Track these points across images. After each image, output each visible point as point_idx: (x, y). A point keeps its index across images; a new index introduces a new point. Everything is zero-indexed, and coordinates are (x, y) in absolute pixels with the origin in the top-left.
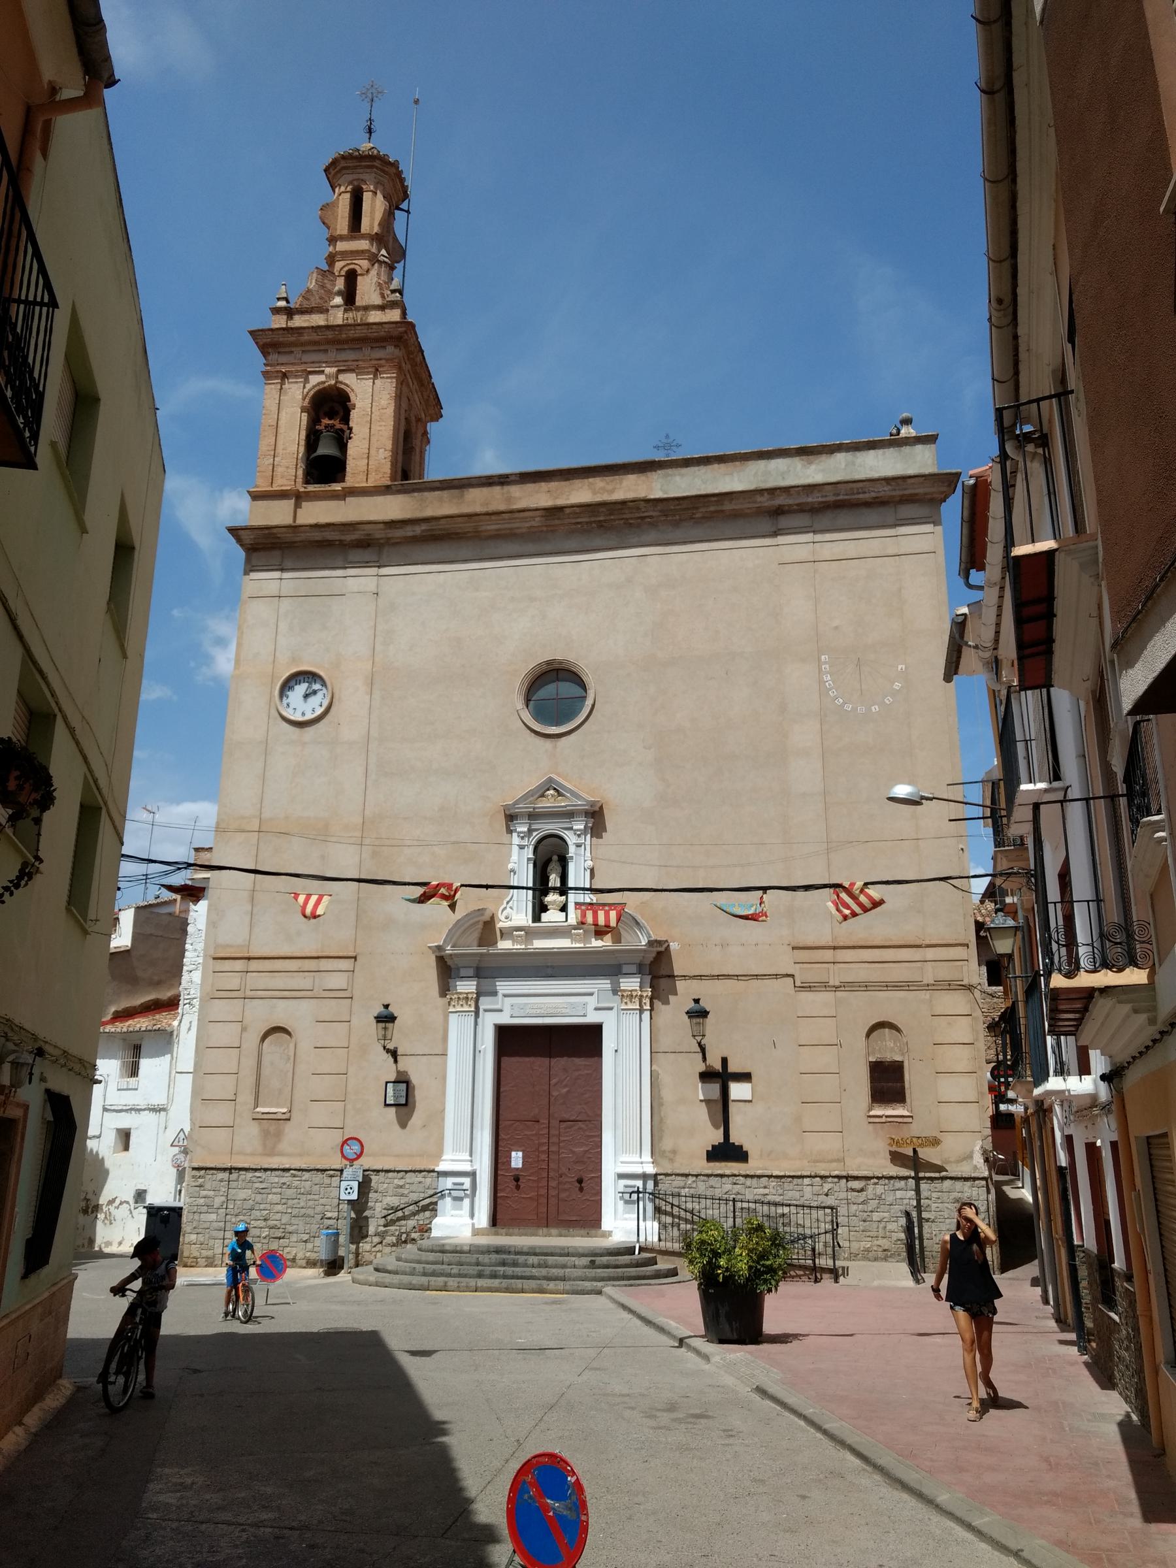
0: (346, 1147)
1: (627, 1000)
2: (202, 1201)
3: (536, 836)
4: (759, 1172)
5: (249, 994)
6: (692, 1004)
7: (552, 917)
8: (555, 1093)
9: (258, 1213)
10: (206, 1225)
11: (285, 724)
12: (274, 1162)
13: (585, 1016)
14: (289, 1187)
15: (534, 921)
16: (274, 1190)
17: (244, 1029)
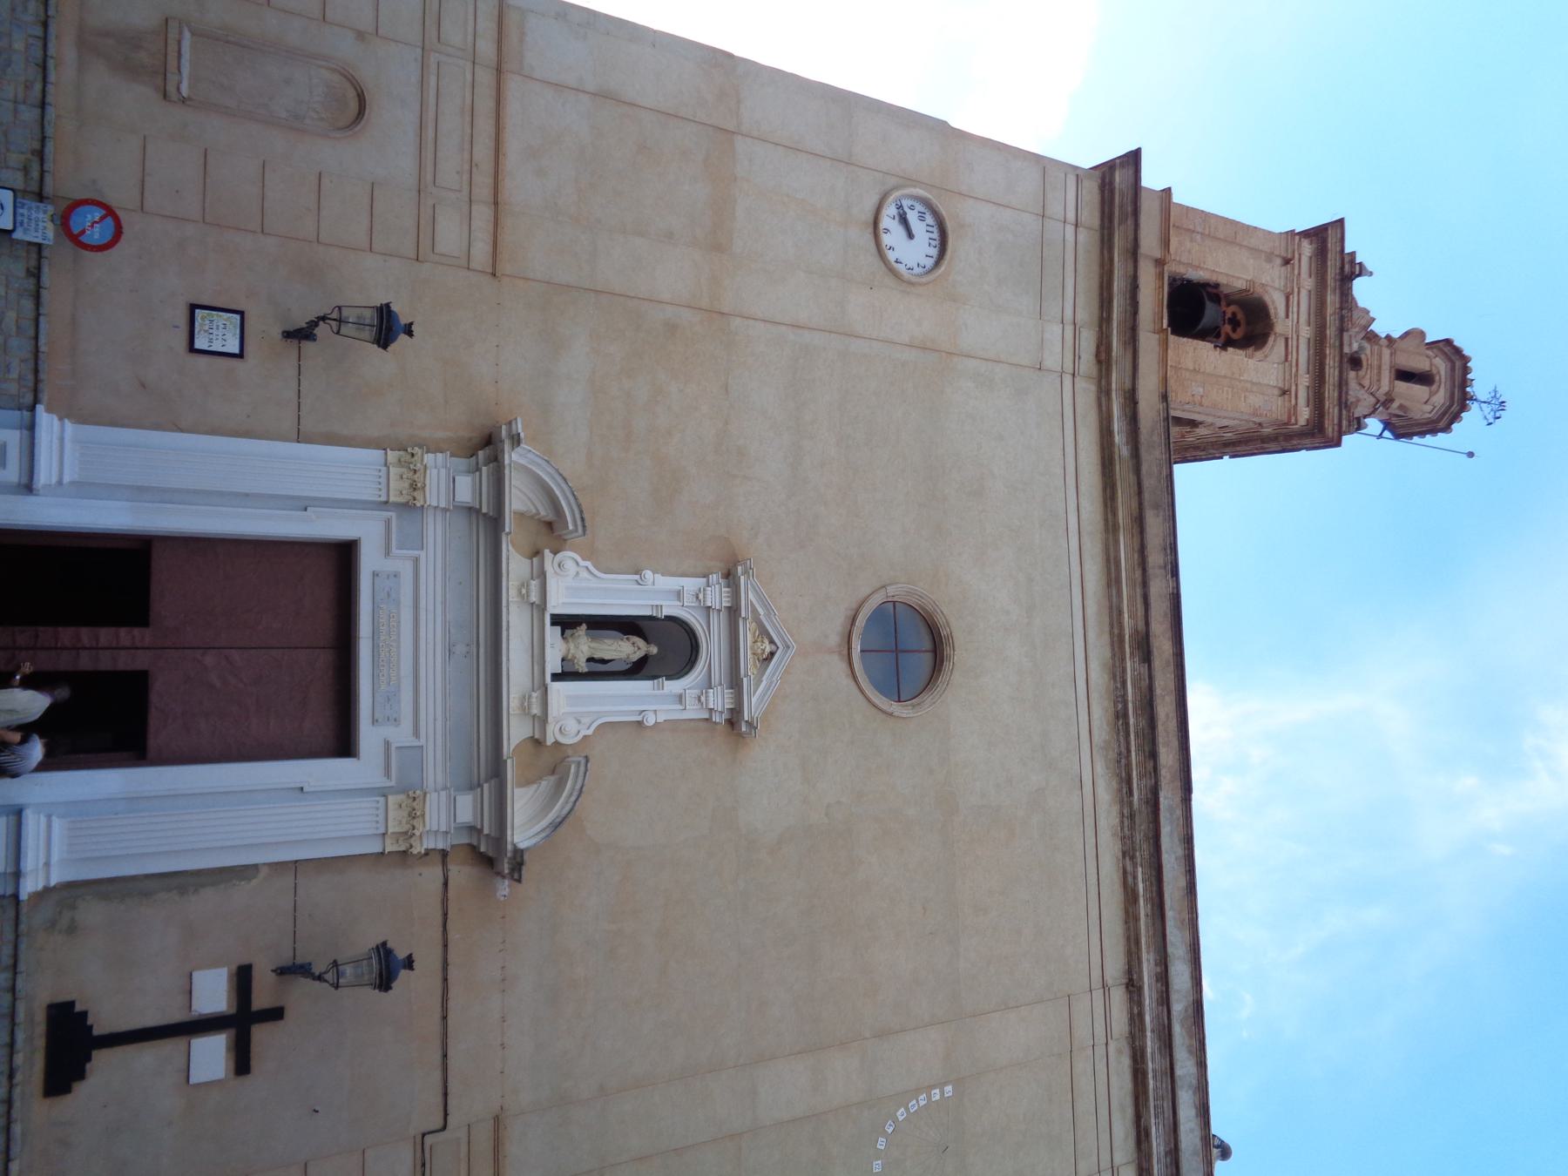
0: (98, 213)
4: (17, 1129)
5: (433, 59)
6: (401, 954)
7: (556, 648)
8: (210, 659)
11: (875, 199)
12: (65, 50)
13: (374, 721)
15: (553, 616)
17: (360, 35)
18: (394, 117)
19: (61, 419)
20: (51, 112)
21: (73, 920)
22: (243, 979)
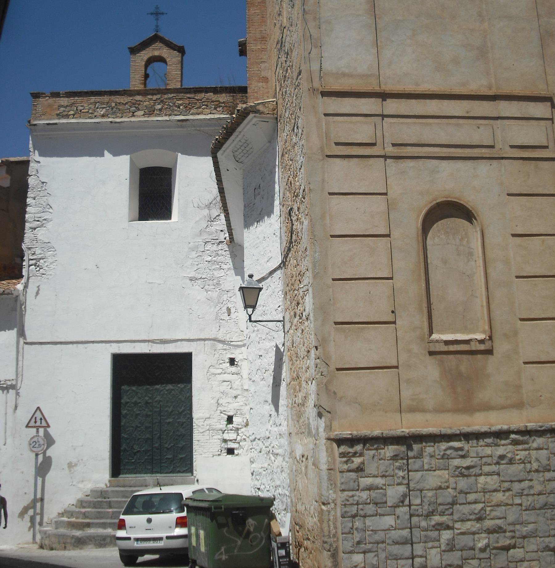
2: (364, 495)
5: (390, 150)
9: (466, 509)
10: (377, 537)
12: (479, 422)
14: (511, 462)
16: (486, 469)
18: (451, 180)
20: (531, 425)
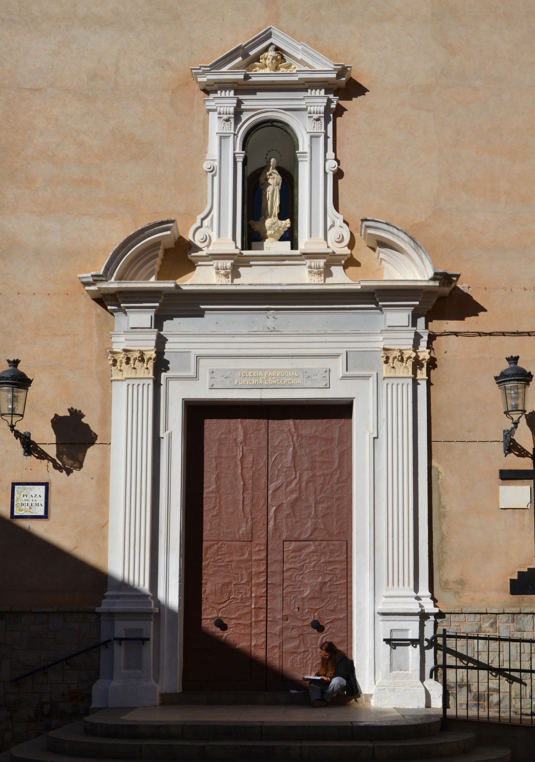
1: (397, 363)
3: (248, 120)
19: (105, 598)
21: (455, 582)
22: (508, 476)
